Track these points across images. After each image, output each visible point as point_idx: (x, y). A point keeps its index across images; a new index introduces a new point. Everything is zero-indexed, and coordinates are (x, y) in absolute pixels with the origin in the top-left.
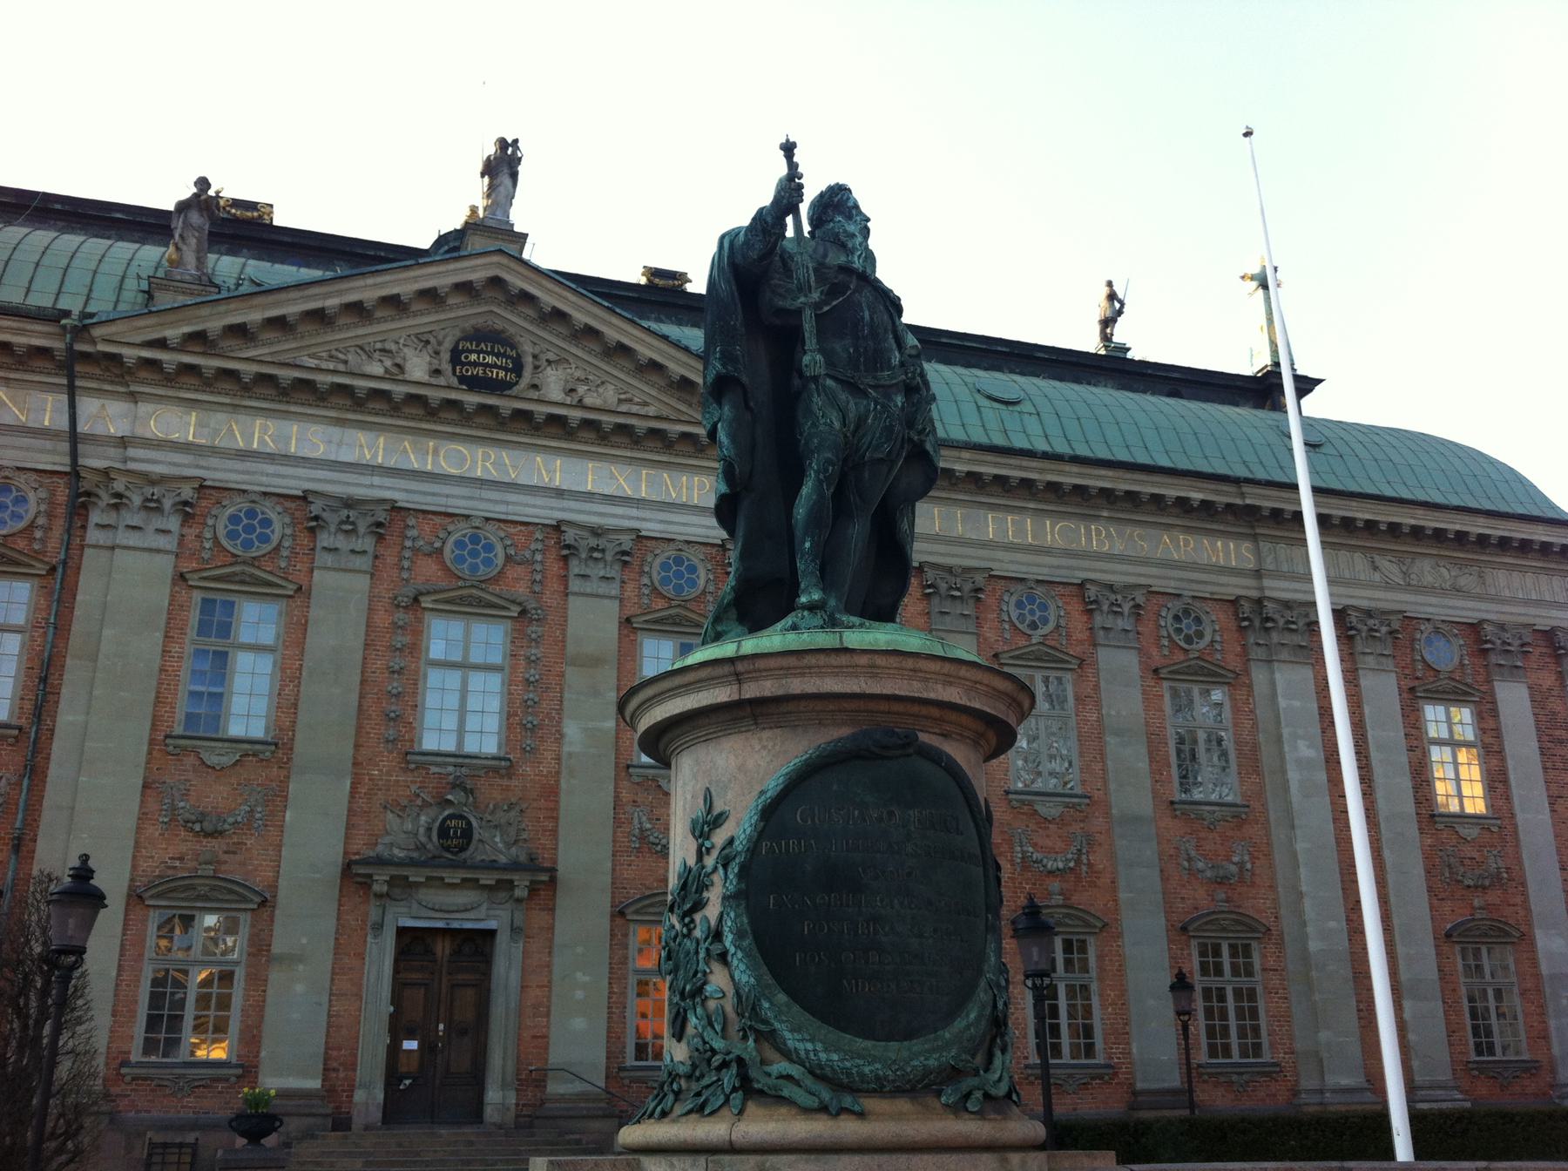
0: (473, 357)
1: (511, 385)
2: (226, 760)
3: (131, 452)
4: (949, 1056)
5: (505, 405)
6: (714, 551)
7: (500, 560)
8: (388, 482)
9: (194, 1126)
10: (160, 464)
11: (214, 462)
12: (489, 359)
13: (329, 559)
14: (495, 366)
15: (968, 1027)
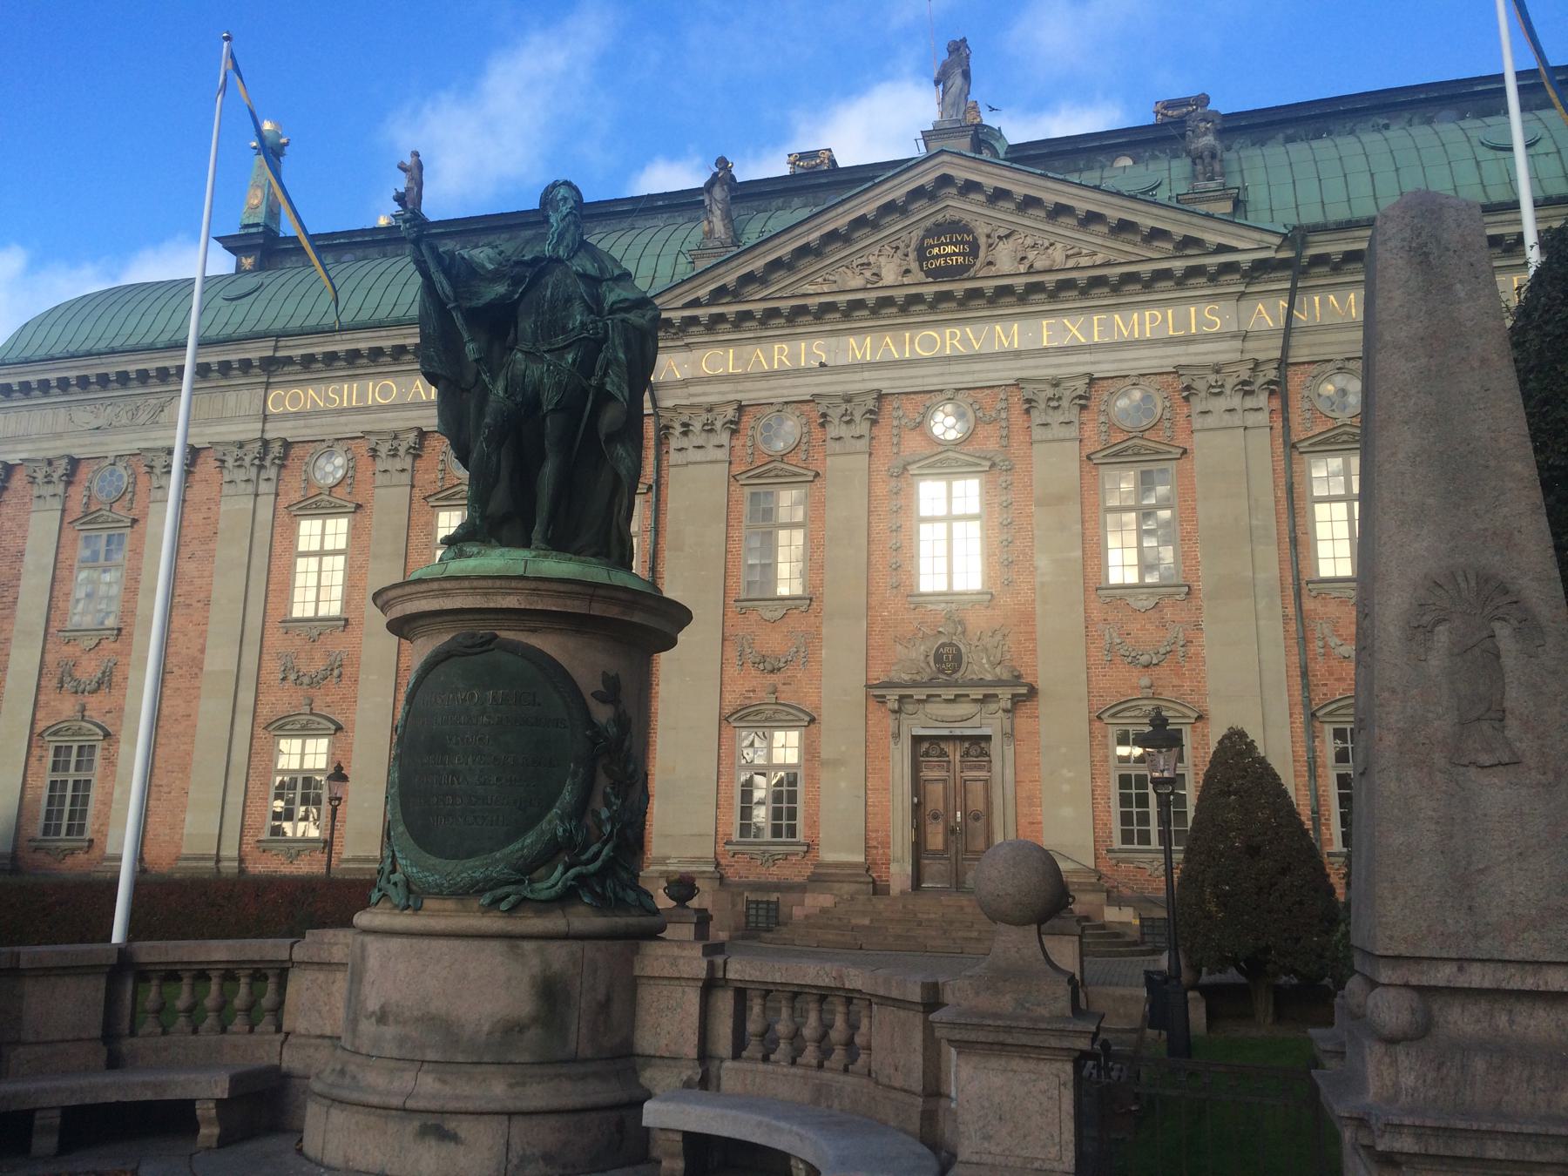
0: (936, 251)
1: (967, 268)
2: (778, 614)
3: (692, 390)
4: (494, 872)
5: (958, 288)
6: (1170, 378)
8: (874, 374)
9: (777, 887)
10: (712, 394)
11: (748, 385)
12: (949, 249)
13: (837, 446)
14: (955, 254)
15: (522, 849)
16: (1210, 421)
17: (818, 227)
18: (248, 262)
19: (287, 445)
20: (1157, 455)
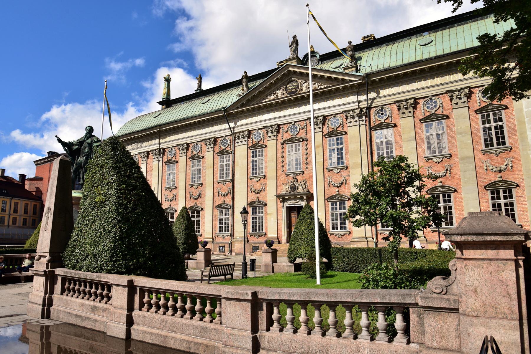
8: (275, 120)
9: (259, 243)
11: (251, 125)
12: (292, 87)
16: (351, 124)
17: (262, 86)
18: (164, 107)
20: (340, 134)
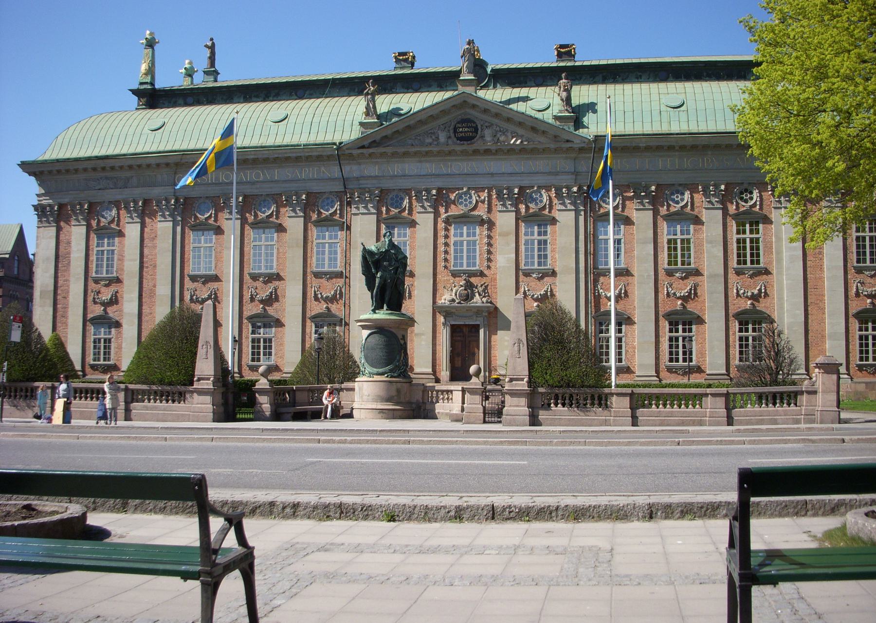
7: (474, 202)
19: (186, 199)
